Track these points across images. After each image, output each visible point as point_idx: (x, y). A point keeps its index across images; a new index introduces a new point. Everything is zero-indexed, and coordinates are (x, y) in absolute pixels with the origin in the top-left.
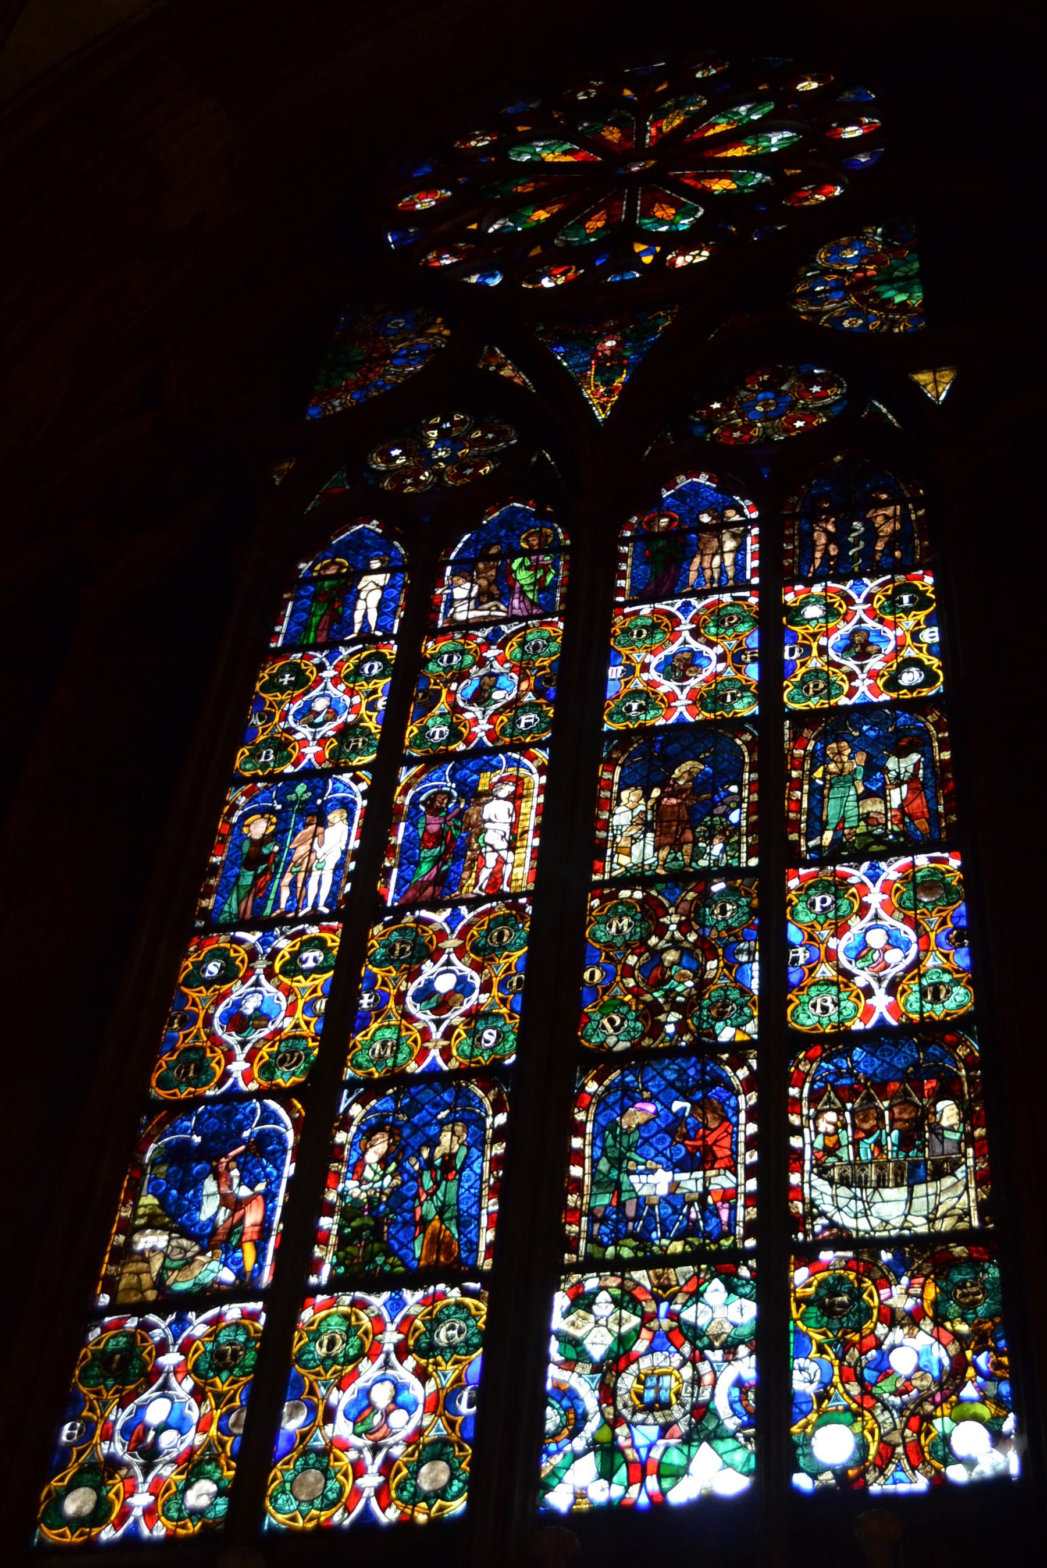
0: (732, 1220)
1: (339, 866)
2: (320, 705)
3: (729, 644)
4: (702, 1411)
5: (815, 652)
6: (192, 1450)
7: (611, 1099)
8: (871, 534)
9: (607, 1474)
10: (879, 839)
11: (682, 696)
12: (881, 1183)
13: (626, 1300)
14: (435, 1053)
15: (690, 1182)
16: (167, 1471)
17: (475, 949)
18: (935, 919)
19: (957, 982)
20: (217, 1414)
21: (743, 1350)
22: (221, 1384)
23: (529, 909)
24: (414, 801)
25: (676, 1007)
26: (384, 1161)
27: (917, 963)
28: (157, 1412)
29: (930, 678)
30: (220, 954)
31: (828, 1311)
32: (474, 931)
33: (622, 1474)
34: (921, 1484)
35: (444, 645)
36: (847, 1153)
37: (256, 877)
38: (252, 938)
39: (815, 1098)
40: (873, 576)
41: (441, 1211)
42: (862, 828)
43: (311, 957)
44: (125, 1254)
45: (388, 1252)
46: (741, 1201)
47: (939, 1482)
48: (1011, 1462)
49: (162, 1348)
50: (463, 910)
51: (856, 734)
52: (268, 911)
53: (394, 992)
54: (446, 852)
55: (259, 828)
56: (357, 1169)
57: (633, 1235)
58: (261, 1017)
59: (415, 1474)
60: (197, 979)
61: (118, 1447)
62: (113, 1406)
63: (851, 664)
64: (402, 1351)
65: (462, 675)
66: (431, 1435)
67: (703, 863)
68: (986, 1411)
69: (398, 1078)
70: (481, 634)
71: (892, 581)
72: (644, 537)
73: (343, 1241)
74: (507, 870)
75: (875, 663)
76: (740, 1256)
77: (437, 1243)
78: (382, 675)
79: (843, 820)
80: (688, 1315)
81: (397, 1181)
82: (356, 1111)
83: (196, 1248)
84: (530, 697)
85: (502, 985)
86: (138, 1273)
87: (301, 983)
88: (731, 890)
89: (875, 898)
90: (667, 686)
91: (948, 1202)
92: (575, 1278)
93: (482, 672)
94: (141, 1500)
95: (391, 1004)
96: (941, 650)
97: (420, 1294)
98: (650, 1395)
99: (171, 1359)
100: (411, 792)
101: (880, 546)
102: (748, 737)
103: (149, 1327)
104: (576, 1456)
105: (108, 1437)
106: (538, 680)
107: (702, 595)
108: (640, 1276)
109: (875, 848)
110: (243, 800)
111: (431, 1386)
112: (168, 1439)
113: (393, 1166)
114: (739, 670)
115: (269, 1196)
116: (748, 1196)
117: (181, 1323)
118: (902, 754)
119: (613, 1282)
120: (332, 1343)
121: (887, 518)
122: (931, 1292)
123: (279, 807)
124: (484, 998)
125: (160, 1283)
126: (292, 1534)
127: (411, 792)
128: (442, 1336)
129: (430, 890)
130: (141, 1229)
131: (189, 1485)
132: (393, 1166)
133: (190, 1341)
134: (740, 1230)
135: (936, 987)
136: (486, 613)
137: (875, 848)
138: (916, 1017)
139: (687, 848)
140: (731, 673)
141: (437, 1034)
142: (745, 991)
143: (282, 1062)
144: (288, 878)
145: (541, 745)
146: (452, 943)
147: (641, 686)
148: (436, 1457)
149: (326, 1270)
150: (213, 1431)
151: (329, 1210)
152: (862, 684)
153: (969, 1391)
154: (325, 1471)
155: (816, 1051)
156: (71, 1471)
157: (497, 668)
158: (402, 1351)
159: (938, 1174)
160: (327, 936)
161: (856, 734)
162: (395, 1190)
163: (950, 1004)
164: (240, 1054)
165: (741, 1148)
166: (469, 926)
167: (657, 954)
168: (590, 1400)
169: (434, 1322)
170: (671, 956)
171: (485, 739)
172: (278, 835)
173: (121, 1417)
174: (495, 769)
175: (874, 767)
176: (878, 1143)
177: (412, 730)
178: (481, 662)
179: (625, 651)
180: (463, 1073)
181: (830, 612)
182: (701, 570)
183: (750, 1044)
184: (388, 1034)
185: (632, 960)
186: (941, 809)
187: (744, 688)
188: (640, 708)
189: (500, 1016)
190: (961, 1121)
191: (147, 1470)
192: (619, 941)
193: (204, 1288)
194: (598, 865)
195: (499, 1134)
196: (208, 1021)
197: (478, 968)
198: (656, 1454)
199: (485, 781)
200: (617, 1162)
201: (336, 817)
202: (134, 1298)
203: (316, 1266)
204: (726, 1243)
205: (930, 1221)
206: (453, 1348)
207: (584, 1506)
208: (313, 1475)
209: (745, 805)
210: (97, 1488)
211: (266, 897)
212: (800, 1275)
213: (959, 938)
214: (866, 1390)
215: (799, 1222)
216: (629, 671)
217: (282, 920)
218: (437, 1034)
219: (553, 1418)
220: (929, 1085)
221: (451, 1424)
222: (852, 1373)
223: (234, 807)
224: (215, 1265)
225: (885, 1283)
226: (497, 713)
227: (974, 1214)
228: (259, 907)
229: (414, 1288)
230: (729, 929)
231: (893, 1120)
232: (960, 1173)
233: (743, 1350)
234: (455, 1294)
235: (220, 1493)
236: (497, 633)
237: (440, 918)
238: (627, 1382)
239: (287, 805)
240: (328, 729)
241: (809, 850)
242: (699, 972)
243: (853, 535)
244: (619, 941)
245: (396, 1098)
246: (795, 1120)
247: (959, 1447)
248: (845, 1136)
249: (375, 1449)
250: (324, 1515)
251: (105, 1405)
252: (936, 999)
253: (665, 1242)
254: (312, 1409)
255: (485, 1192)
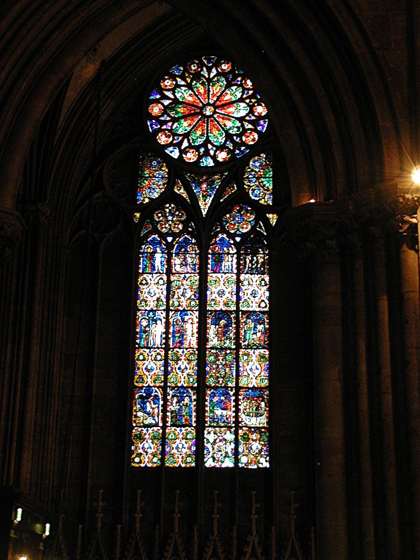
0: (231, 421)
1: (161, 336)
2: (152, 291)
3: (230, 289)
4: (227, 453)
5: (246, 294)
6: (153, 452)
7: (212, 395)
8: (257, 262)
9: (214, 461)
10: (255, 345)
11: (221, 301)
12: (253, 416)
13: (215, 433)
14: (182, 382)
15: (225, 412)
16: (150, 456)
17: (188, 360)
18: (263, 364)
19: (266, 379)
20: (156, 446)
21: (232, 443)
22: (155, 441)
23: (197, 352)
24: (173, 322)
25: (222, 377)
26: (176, 403)
27: (260, 374)
28: (146, 446)
29: (266, 307)
30: (141, 354)
31: (244, 438)
32: (187, 355)
33: (216, 461)
34: (255, 467)
35: (175, 278)
36: (248, 410)
37: (146, 336)
38: (148, 351)
39: (243, 399)
40: (257, 274)
41: (186, 414)
42: (252, 342)
43: (159, 357)
44: (136, 416)
45: (179, 420)
46: (232, 417)
47: (258, 467)
48: (267, 465)
49: (145, 434)
50: (185, 350)
51: (252, 318)
52: (149, 345)
53: (174, 367)
54: (180, 335)
55: (144, 323)
56: (172, 403)
57: (216, 422)
58: (152, 370)
59: (186, 459)
60: (138, 360)
61: (141, 451)
62: (139, 444)
63: (252, 299)
64: (183, 439)
65: (179, 288)
66: (188, 453)
67: (226, 345)
68: (265, 456)
69: (177, 386)
70: (183, 276)
71: (261, 277)
72: (213, 254)
73: (172, 418)
74: (192, 342)
75: (257, 299)
76: (232, 427)
77: (186, 420)
78: (163, 285)
79: (249, 339)
80: (225, 437)
81: (179, 407)
82: (171, 392)
83: (148, 416)
84: (193, 297)
85: (193, 368)
86: (139, 420)
87: (158, 363)
88: (231, 353)
89: (254, 358)
90: (219, 299)
91: (262, 421)
92: (208, 428)
93: (183, 288)
94: (146, 460)
95: (174, 370)
96: (270, 299)
97: (185, 429)
98: (219, 449)
99: (147, 437)
100: (173, 318)
101: (259, 266)
102: (233, 315)
103: (142, 430)
104: (209, 458)
105: (139, 449)
106: (195, 292)
107: (225, 273)
108: (217, 429)
109: (255, 347)
110: (140, 315)
111: (188, 445)
112: (149, 450)
113: (178, 404)
114: (232, 297)
115: (158, 407)
116: (233, 416)
117: (148, 430)
118: (260, 324)
119: (213, 430)
120: (172, 436)
121: (261, 257)
122: (259, 436)
123: (147, 318)
124: (190, 371)
125: (143, 422)
126: (169, 467)
127: (173, 318)
128: (188, 437)
129: (178, 344)
130: (138, 412)
131: (153, 458)
132: (178, 404)
133: (150, 433)
134: (232, 422)
135: (263, 379)
136: (183, 270)
137: (255, 347)
138: (259, 385)
139: (223, 341)
140: (230, 297)
141: (182, 377)
142: (233, 376)
143: (157, 380)
144: (152, 337)
145: (196, 311)
146: (183, 358)
147: (214, 298)
148: (190, 457)
149: (169, 423)
150: (156, 450)
151: (168, 411)
152: (254, 304)
153: (263, 453)
154: (173, 457)
155: (244, 390)
156: (135, 455)
157: (187, 287)
158: (183, 439)
159: (261, 416)
160: (160, 352)
161: (252, 318)
162: (179, 409)
163: (265, 383)
164: (149, 377)
165: (232, 407)
166: (186, 354)
167: (218, 365)
168: (211, 449)
169: (187, 434)
170: (221, 366)
171: (185, 307)
172: (148, 326)
173: (141, 446)
174: (188, 315)
175: (255, 327)
176: (252, 409)
177: (171, 302)
178: (183, 285)
179: (210, 287)
180: (188, 387)
181: (249, 284)
182: (225, 266)
183: (234, 387)
184: (174, 376)
185: (214, 366)
186: (266, 340)
187: (233, 302)
188: (214, 304)
189: (193, 376)
190: (265, 406)
191: (147, 455)
192: (212, 362)
193: (151, 424)
194: (207, 343)
195: (195, 400)
196: (142, 370)
197: (188, 364)
198: (220, 459)
199: (186, 318)
200: (213, 407)
201: (159, 322)
202: (139, 425)
203: (167, 422)
204: (230, 425)
205: (259, 424)
206: (190, 439)
207: (210, 466)
208: (172, 458)
209: (233, 333)
210: (140, 457)
211: (148, 341)
212: (240, 431)
213: (267, 369)
214: (249, 451)
215: (240, 422)
216: (211, 293)
217: (152, 348)
218: (182, 377)
219: (206, 452)
220: (261, 399)
221: (191, 452)
222: (247, 449)
223: (139, 317)
224: (151, 420)
225: (252, 434)
226: (187, 300)
227: (266, 423)
228: (147, 344)
229: (184, 427)
230: (230, 361)
231: (255, 406)
232: (264, 416)
233: (232, 443)
234: (189, 429)
235: (158, 460)
236: (185, 277)
237: (180, 351)
238: (216, 447)
239: (149, 318)
240: (155, 298)
241: (244, 345)
242: (225, 370)
243: (254, 261)
244: (212, 362)
245: (177, 390)
246: (240, 403)
247: (261, 461)
248: (248, 407)
249: (180, 455)
250: (174, 464)
251: (138, 443)
252: (262, 382)
253: (221, 423)
254: (170, 447)
255: (193, 411)
